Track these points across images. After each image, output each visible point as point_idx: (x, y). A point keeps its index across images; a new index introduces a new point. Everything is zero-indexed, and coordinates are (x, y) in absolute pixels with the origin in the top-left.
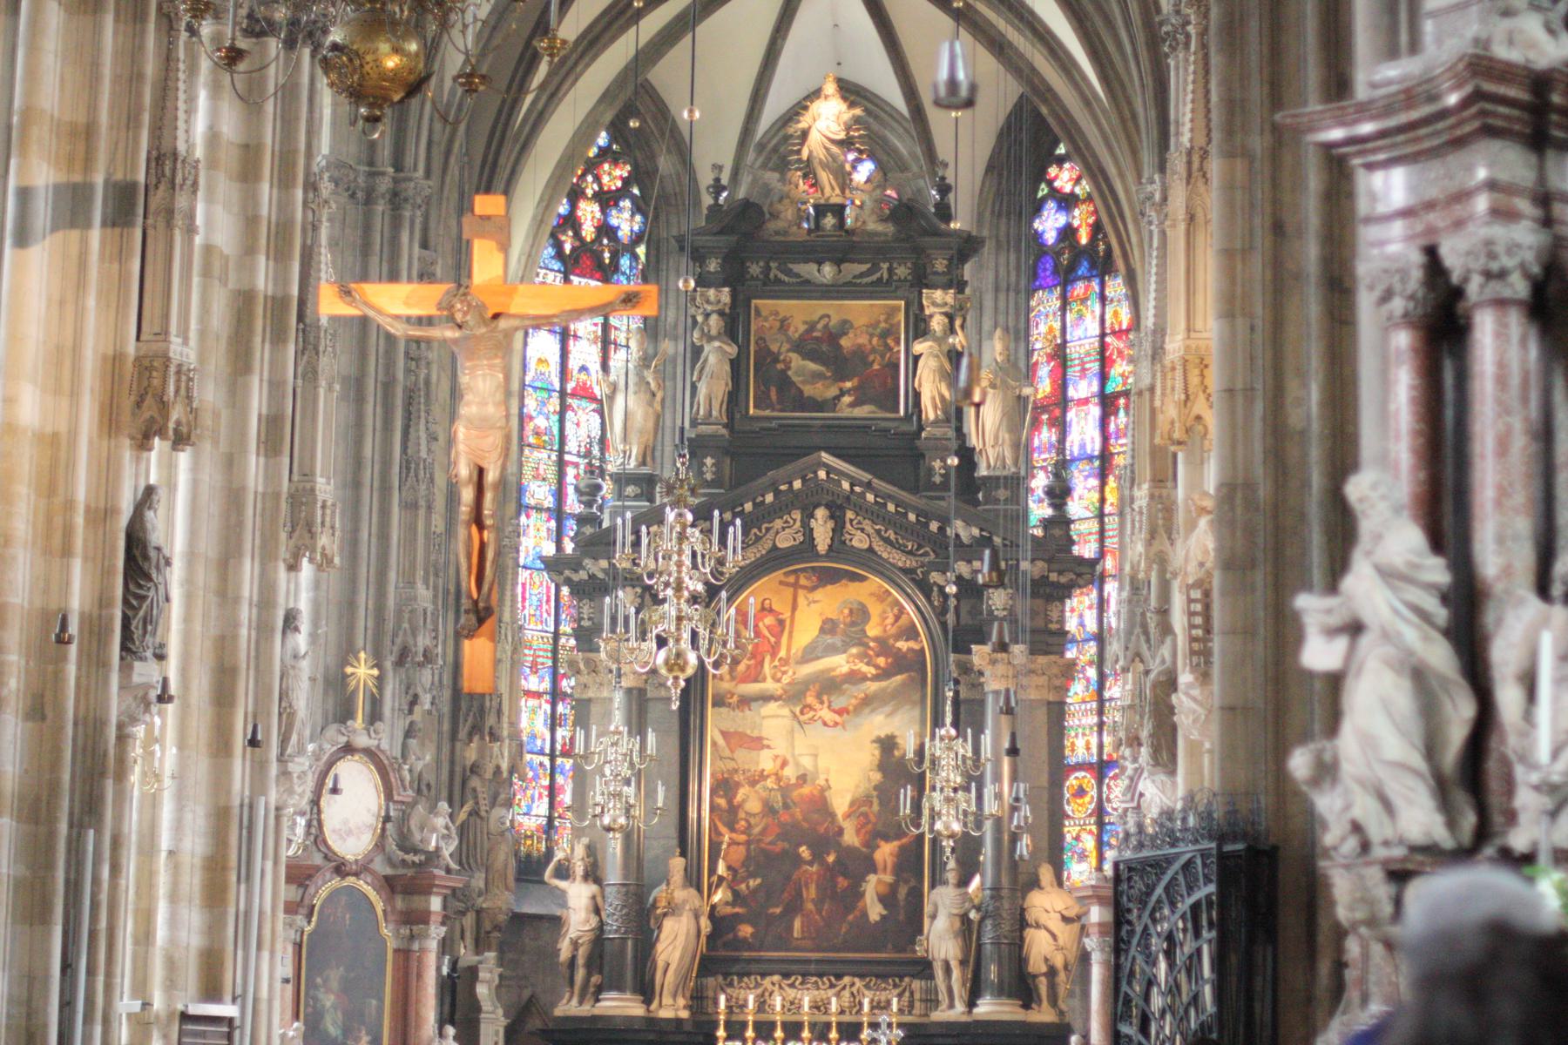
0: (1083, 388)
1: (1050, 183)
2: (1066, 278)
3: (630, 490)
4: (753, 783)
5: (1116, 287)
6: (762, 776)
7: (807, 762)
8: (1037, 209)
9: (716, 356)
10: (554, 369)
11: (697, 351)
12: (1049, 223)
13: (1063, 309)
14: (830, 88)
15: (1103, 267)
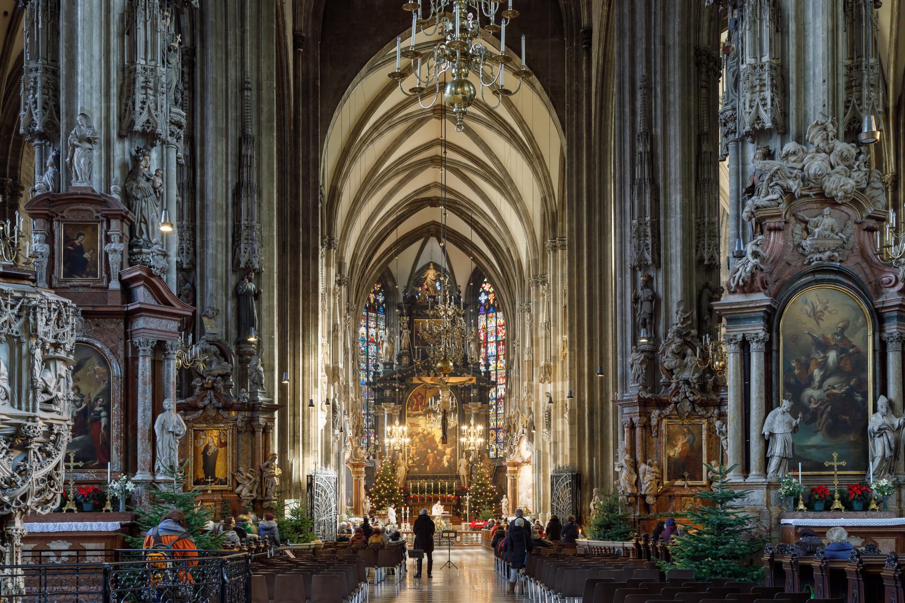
0: (492, 339)
1: (483, 288)
2: (487, 312)
3: (388, 367)
4: (417, 435)
5: (500, 315)
6: (419, 433)
7: (429, 430)
8: (480, 294)
9: (406, 333)
10: (365, 336)
11: (401, 332)
12: (483, 298)
13: (487, 320)
14: (431, 267)
15: (497, 310)
